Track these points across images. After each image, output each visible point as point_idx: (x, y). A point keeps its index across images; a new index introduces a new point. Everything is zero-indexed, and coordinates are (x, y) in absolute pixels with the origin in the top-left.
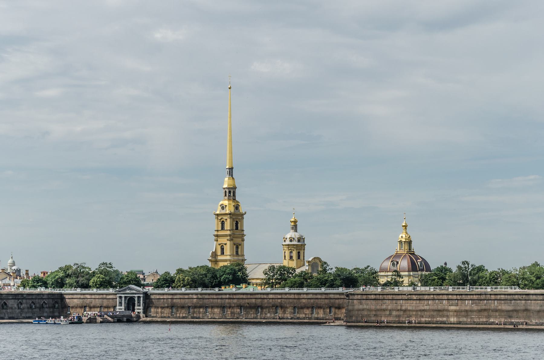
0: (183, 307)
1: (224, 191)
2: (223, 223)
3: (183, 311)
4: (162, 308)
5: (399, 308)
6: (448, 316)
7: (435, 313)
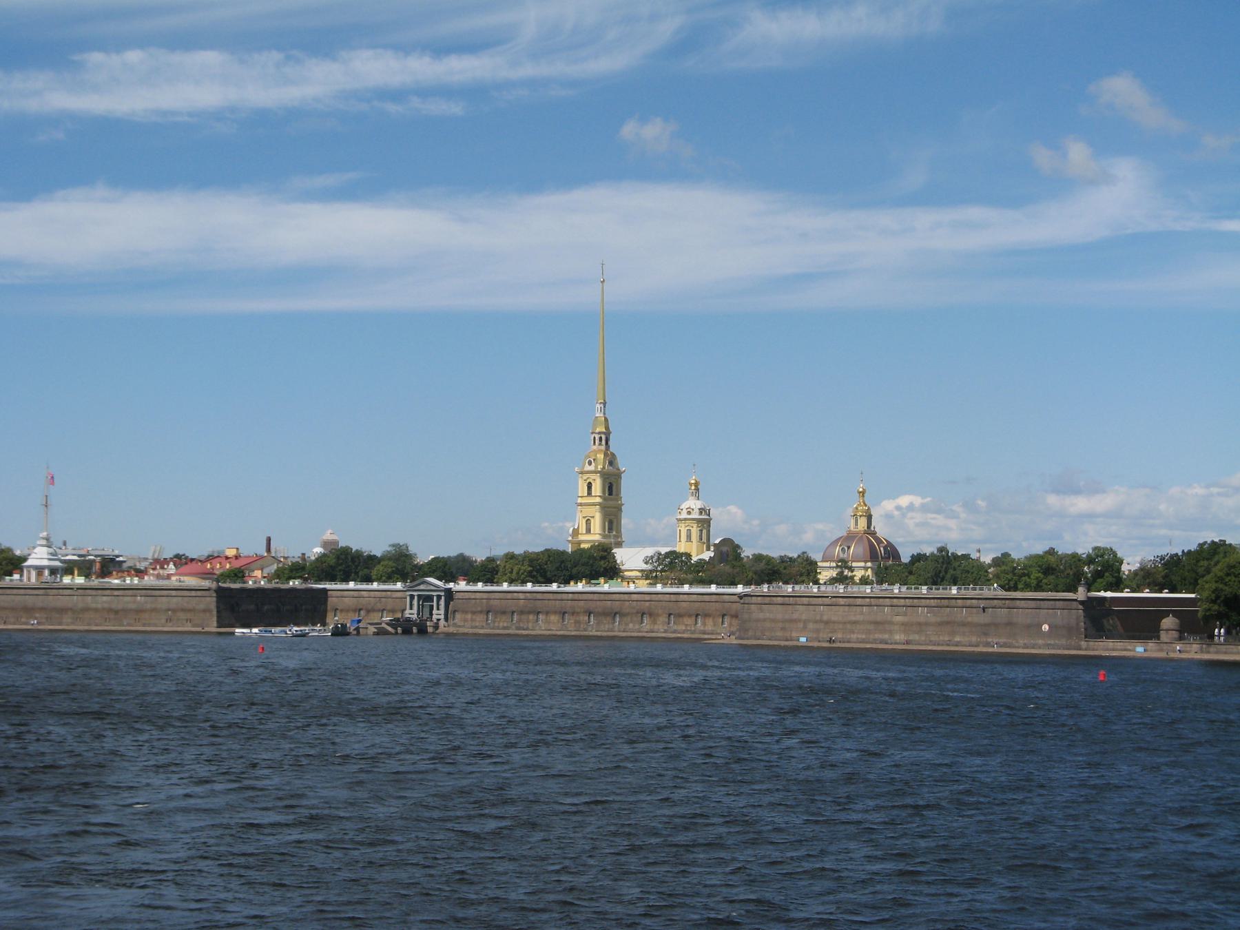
0: (504, 613)
2: (590, 486)
3: (504, 618)
4: (474, 613)
5: (818, 618)
6: (891, 632)
7: (871, 627)
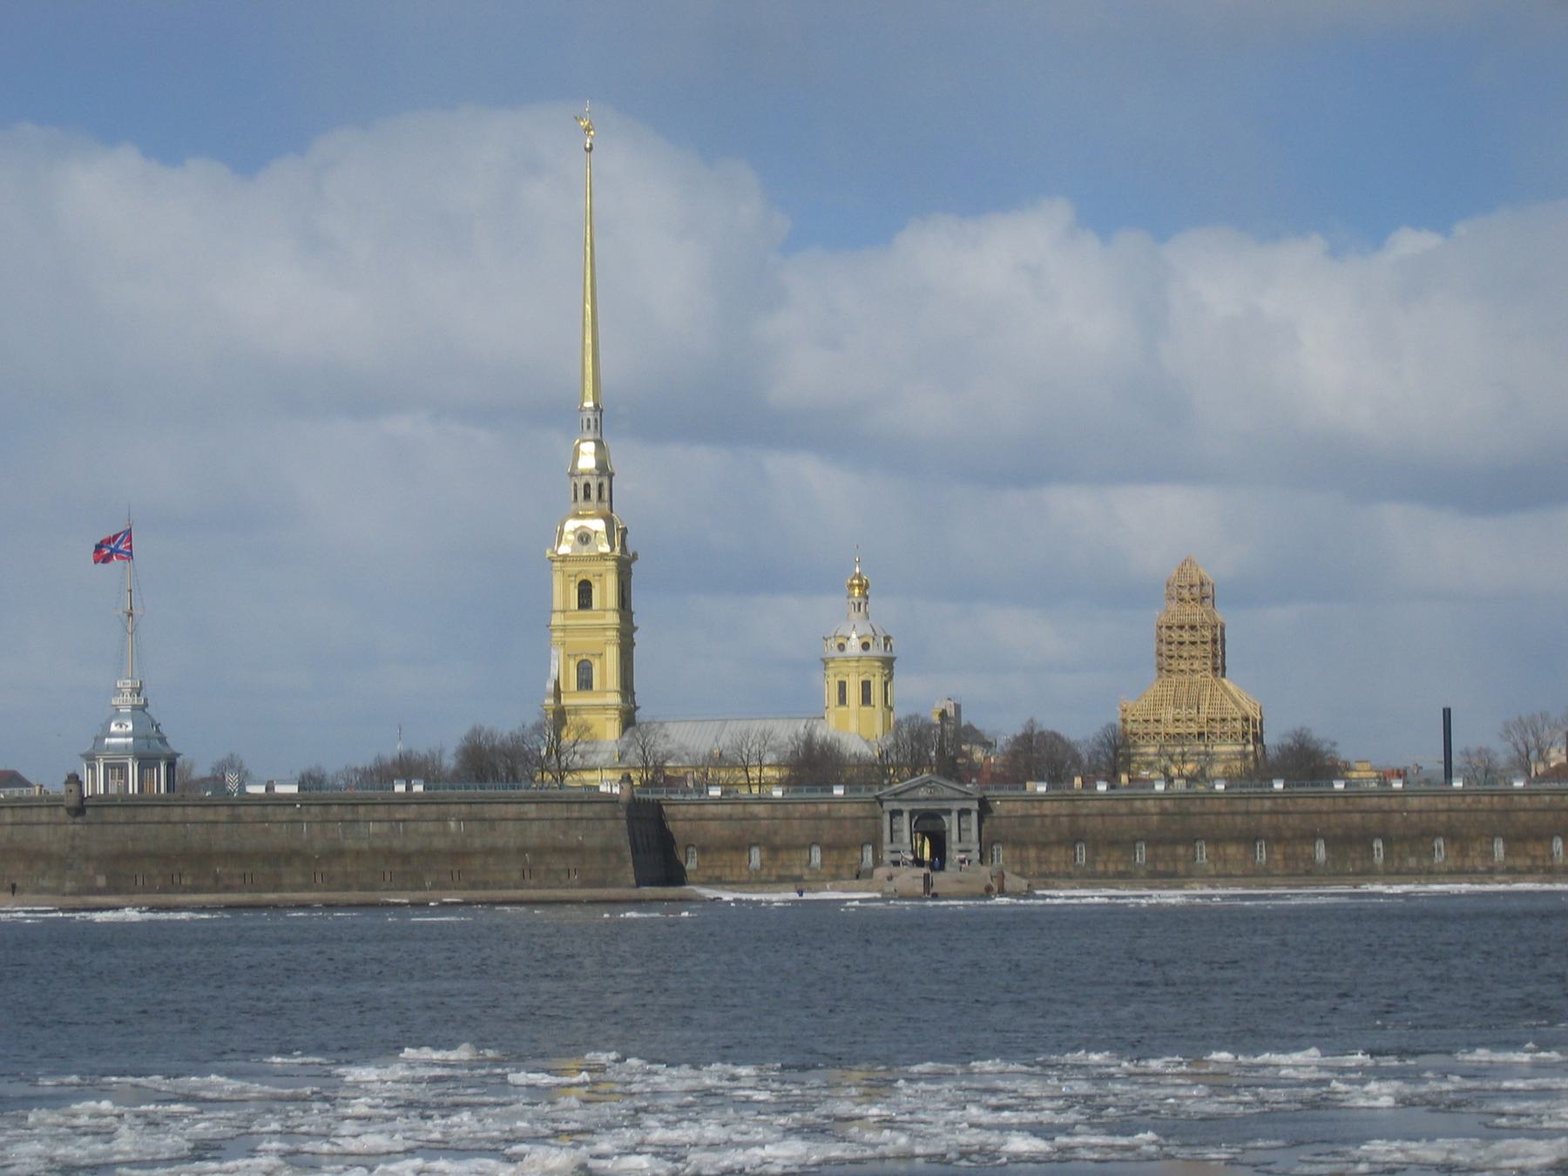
0: (1114, 843)
2: (585, 590)
4: (1042, 845)
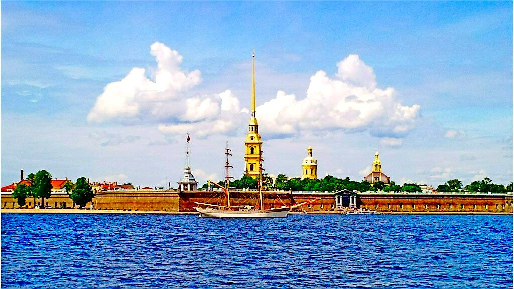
1: (251, 127)
4: (369, 205)
